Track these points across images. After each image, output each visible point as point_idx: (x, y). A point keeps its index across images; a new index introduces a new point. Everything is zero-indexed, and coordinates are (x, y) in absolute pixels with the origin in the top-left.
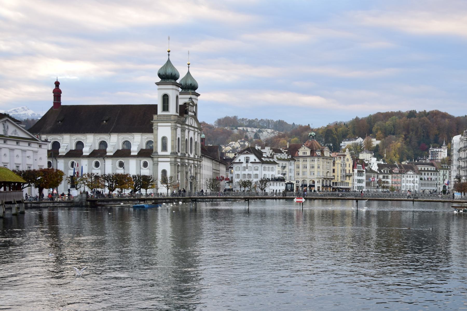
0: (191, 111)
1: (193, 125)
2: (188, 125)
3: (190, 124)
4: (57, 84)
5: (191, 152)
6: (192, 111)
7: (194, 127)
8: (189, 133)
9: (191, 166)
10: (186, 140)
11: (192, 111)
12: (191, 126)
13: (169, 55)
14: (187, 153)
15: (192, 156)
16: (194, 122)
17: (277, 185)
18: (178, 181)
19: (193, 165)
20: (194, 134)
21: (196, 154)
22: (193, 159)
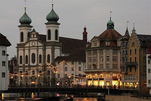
0: (34, 37)
1: (36, 45)
2: (30, 47)
3: (31, 46)
4: (85, 29)
5: (33, 61)
6: (35, 37)
7: (38, 46)
8: (29, 51)
9: (33, 72)
10: (27, 56)
11: (35, 37)
12: (34, 46)
13: (25, 10)
14: (27, 63)
15: (35, 64)
16: (37, 43)
17: (82, 81)
18: (19, 81)
19: (36, 70)
20: (38, 51)
21: (40, 62)
22: (37, 66)
